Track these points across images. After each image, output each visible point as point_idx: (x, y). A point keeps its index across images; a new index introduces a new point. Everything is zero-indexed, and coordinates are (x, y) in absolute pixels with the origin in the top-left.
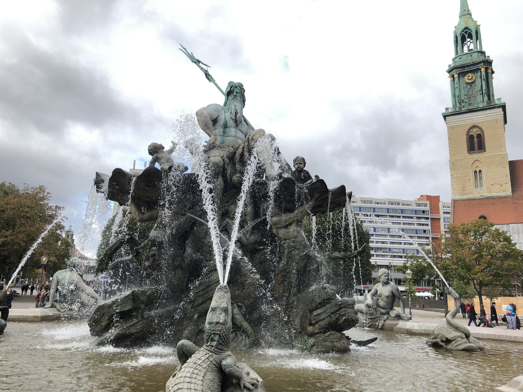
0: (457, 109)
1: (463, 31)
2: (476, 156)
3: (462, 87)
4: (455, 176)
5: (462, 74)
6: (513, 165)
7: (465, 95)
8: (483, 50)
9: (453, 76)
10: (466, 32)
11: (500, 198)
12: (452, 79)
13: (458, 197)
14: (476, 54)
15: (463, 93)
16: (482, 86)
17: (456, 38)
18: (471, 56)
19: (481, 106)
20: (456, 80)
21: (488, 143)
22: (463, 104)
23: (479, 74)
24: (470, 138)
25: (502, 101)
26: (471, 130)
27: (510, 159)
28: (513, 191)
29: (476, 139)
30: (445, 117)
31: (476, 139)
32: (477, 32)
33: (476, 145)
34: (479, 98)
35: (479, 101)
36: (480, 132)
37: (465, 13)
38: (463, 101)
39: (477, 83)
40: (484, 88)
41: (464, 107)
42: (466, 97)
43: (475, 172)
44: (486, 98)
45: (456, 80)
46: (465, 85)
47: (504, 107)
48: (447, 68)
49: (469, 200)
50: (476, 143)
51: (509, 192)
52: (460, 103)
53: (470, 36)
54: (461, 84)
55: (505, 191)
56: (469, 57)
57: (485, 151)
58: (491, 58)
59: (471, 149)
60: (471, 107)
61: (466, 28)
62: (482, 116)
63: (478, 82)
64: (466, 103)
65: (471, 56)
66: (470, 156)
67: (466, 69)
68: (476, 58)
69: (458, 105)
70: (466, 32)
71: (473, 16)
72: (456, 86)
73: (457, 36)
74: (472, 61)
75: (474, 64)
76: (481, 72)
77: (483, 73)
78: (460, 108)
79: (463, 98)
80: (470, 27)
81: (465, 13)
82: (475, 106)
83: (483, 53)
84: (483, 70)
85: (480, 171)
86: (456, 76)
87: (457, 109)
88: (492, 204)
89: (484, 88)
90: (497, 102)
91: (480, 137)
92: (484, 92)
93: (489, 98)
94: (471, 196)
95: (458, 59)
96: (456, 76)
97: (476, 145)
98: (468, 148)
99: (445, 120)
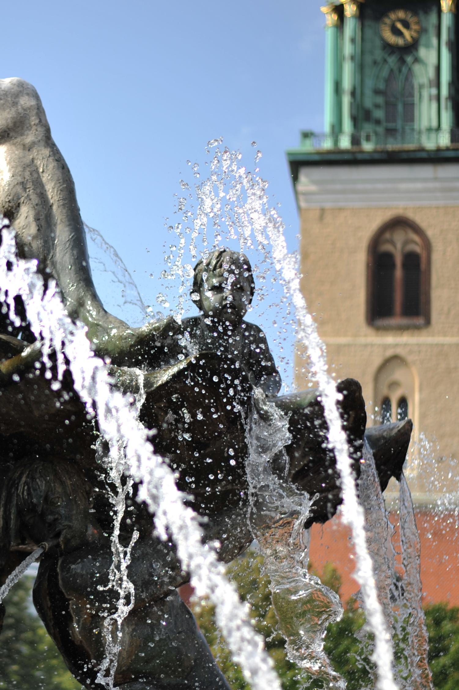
0: (345, 143)
2: (392, 341)
7: (377, 92)
15: (370, 83)
19: (429, 144)
22: (368, 128)
23: (433, 18)
26: (387, 235)
29: (399, 273)
31: (399, 273)
35: (424, 124)
41: (368, 139)
42: (380, 100)
46: (379, 54)
57: (428, 322)
59: (379, 309)
60: (392, 146)
62: (430, 185)
64: (378, 122)
69: (347, 125)
78: (355, 141)
79: (368, 103)
82: (411, 146)
87: (345, 143)
91: (416, 267)
99: (295, 178)
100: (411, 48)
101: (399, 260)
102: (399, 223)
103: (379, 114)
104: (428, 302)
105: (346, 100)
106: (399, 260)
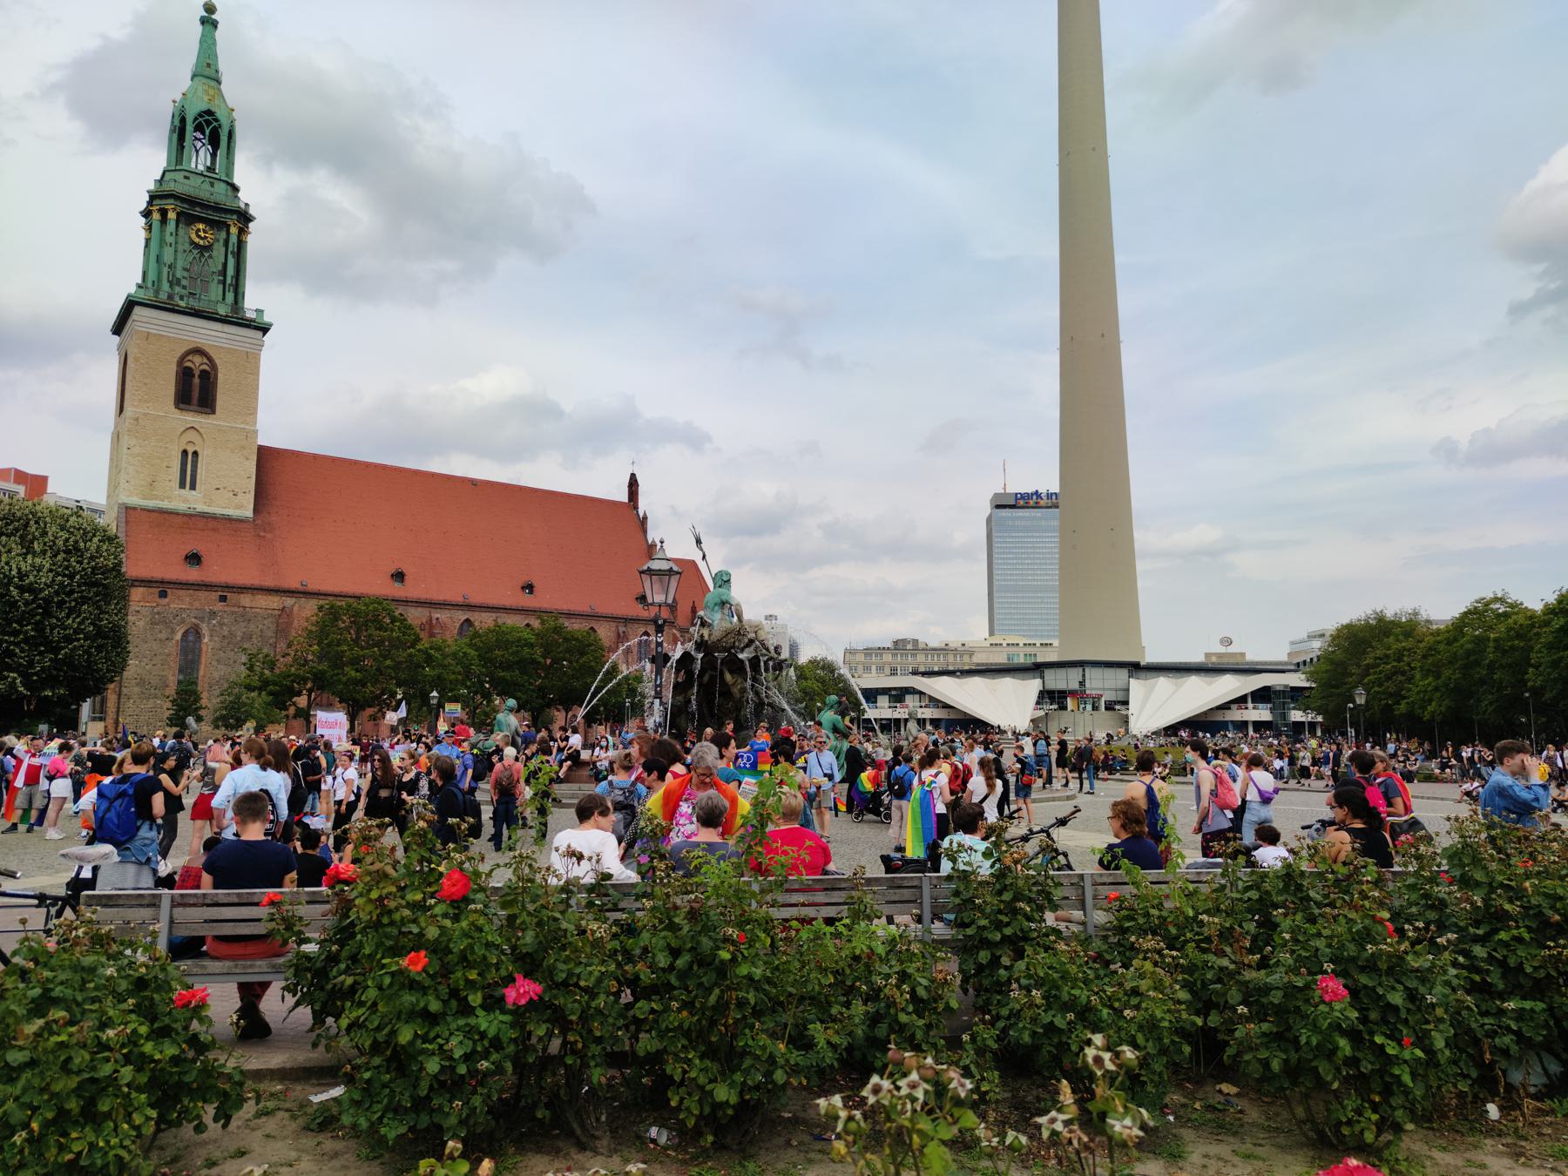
0: (163, 296)
1: (200, 115)
2: (191, 418)
3: (180, 248)
4: (136, 450)
5: (186, 219)
6: (267, 457)
8: (237, 181)
9: (164, 213)
10: (208, 123)
11: (229, 520)
12: (156, 216)
13: (135, 501)
14: (223, 185)
15: (180, 264)
16: (225, 265)
17: (183, 120)
18: (212, 185)
19: (222, 310)
20: (171, 226)
21: (222, 399)
22: (177, 289)
24: (185, 374)
25: (267, 319)
27: (263, 441)
28: (255, 510)
29: (196, 381)
30: (129, 306)
31: (196, 381)
32: (231, 135)
33: (196, 394)
34: (215, 291)
36: (205, 367)
37: (207, 71)
38: (178, 282)
39: (215, 253)
40: (231, 271)
41: (182, 298)
42: (186, 274)
43: (185, 452)
44: (230, 297)
45: (171, 226)
46: (187, 247)
47: (265, 330)
48: (152, 187)
49: (161, 512)
50: (197, 388)
51: (248, 512)
52: (171, 284)
53: (214, 141)
54: (180, 240)
55: (239, 507)
56: (207, 186)
57: (214, 412)
58: (252, 211)
61: (209, 112)
63: (218, 251)
65: (212, 185)
66: (177, 414)
67: (197, 212)
68: (219, 193)
69: (166, 286)
70: (208, 123)
71: (222, 87)
72: (170, 239)
73: (183, 120)
74: (213, 199)
75: (217, 208)
76: (228, 233)
77: (233, 239)
78: (170, 297)
79: (179, 274)
80: (218, 115)
81: (207, 71)
83: (235, 189)
84: (234, 230)
85: (195, 453)
86: (172, 215)
87: (163, 296)
88: (214, 530)
89: (231, 271)
90: (250, 315)
92: (229, 281)
93: (236, 302)
94: (165, 505)
95: (179, 176)
96: (172, 215)
97: (196, 394)
98: (177, 394)
100: (208, 248)
101: (197, 373)
102: (198, 351)
103: (184, 282)
104: (214, 400)
105: (165, 270)
106: (197, 373)
